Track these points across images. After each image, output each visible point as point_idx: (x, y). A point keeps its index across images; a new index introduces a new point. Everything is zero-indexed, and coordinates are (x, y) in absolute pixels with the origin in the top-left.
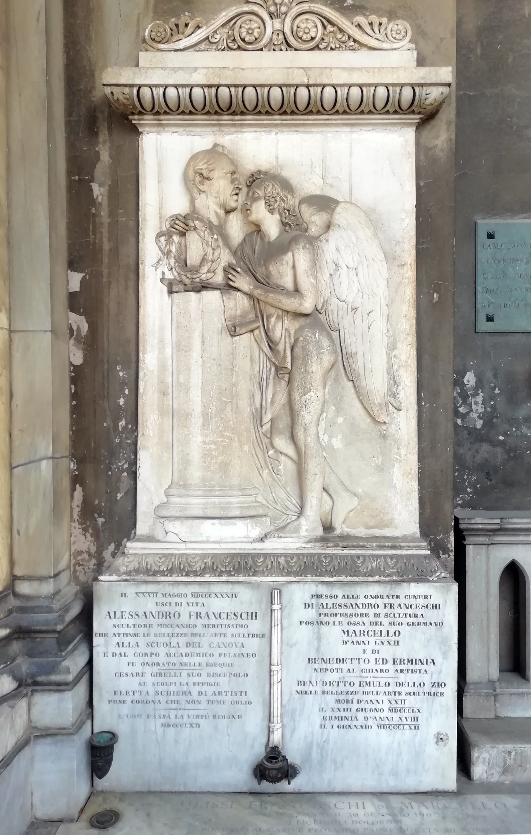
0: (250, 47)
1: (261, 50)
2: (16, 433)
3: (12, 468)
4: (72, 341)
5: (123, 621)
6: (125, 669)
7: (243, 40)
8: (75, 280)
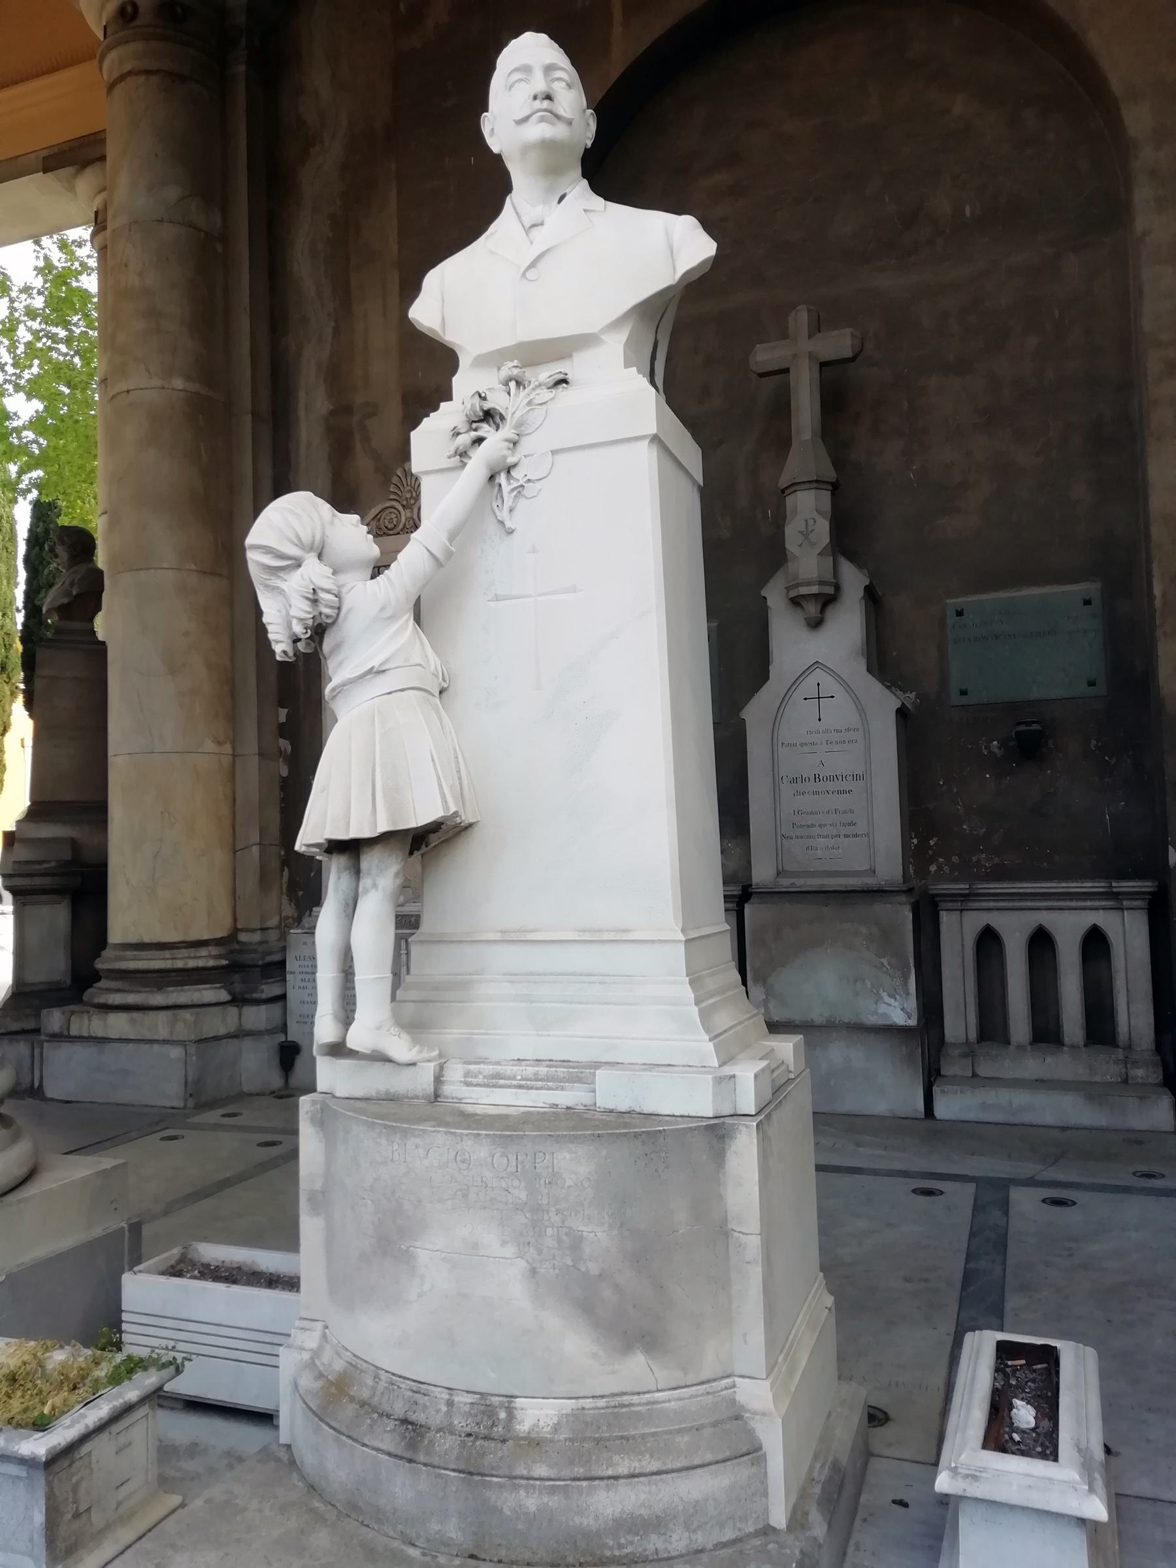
2: (237, 828)
3: (235, 852)
5: (306, 963)
8: (283, 714)
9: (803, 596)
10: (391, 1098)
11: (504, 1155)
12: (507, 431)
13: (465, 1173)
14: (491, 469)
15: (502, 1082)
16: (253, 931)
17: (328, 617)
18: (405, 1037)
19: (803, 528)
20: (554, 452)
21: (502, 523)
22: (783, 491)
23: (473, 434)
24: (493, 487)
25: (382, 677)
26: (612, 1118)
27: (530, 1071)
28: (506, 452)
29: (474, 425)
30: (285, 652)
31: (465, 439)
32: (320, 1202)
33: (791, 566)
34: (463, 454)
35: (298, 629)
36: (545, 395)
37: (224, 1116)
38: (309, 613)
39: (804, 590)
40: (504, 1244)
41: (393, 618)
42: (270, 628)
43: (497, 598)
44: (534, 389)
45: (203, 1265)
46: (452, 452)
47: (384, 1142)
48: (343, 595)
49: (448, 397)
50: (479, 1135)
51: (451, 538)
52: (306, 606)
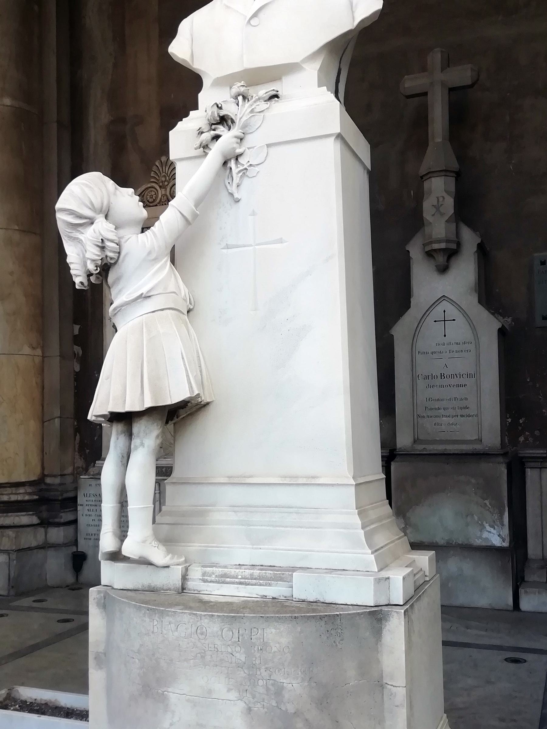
0: (151, 204)
1: (156, 205)
4: (75, 360)
5: (90, 498)
6: (92, 523)
7: (148, 201)
8: (76, 329)
9: (435, 250)
10: (153, 590)
11: (230, 630)
12: (236, 131)
13: (203, 641)
14: (224, 156)
15: (228, 580)
16: (55, 476)
17: (111, 258)
18: (162, 548)
19: (435, 203)
20: (268, 146)
21: (231, 194)
22: (422, 177)
23: (213, 133)
24: (226, 169)
25: (149, 300)
26: (304, 605)
27: (248, 572)
28: (235, 145)
29: (213, 127)
30: (82, 283)
31: (207, 136)
32: (103, 660)
33: (427, 229)
34: (205, 147)
35: (91, 267)
36: (263, 105)
37: (34, 601)
38: (99, 256)
39: (436, 246)
40: (229, 690)
41: (156, 260)
42: (71, 266)
43: (228, 247)
44: (255, 102)
45: (22, 701)
46: (198, 145)
47: (147, 619)
48: (122, 243)
49: (196, 107)
50: (213, 615)
51: (197, 204)
52: (97, 251)
